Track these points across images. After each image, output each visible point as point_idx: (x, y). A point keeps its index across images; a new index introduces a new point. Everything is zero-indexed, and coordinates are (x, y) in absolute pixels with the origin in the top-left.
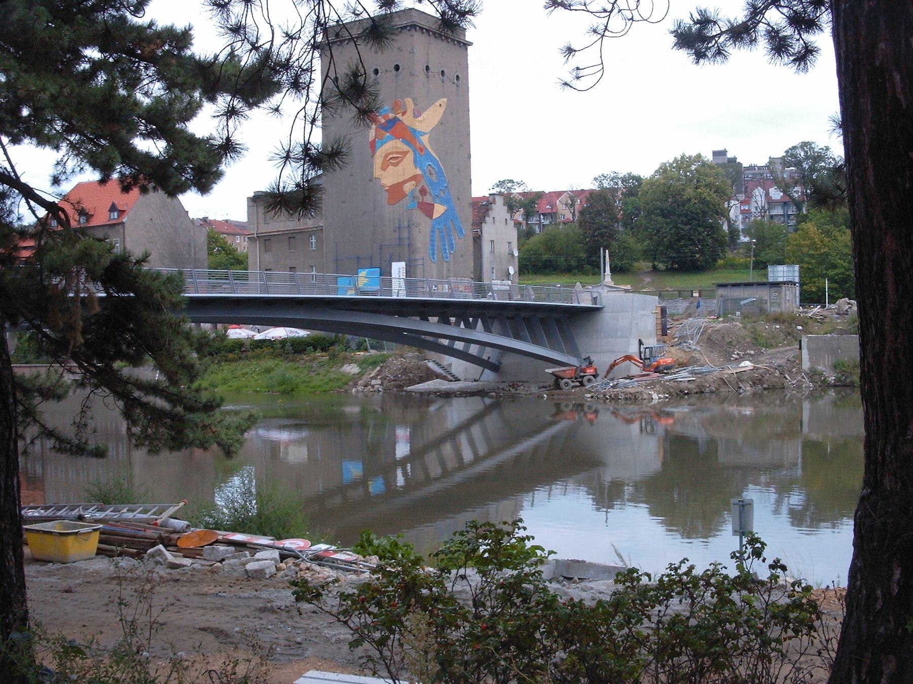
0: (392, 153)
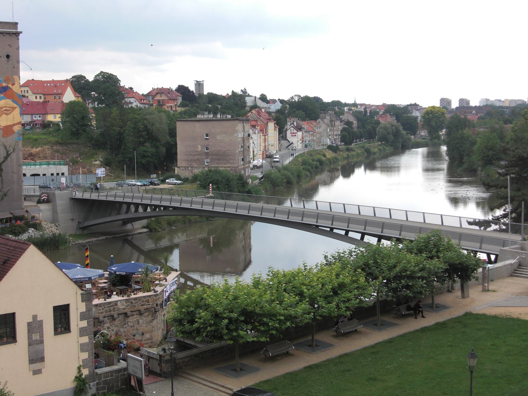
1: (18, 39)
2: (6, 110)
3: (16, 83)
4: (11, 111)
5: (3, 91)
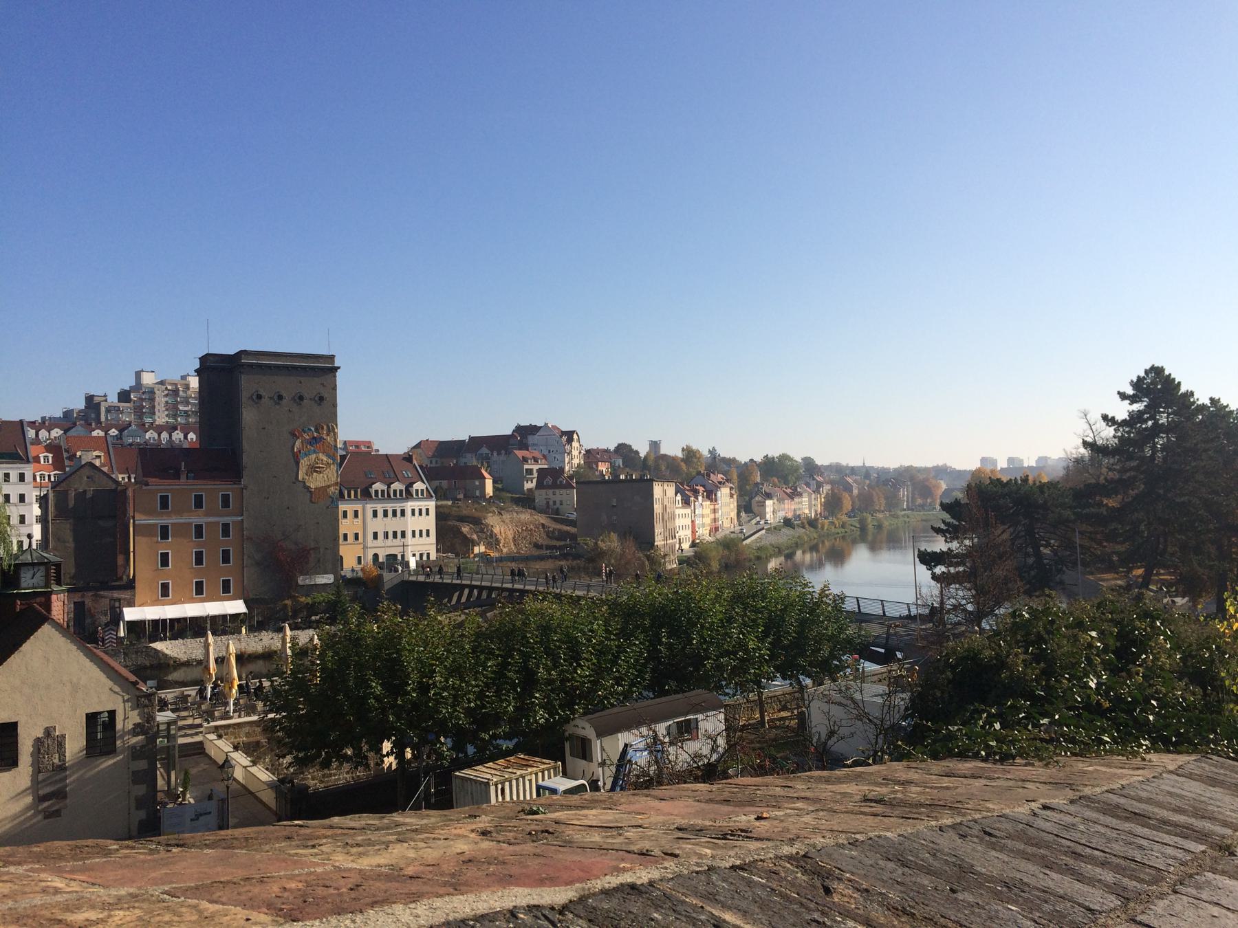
1: (335, 376)
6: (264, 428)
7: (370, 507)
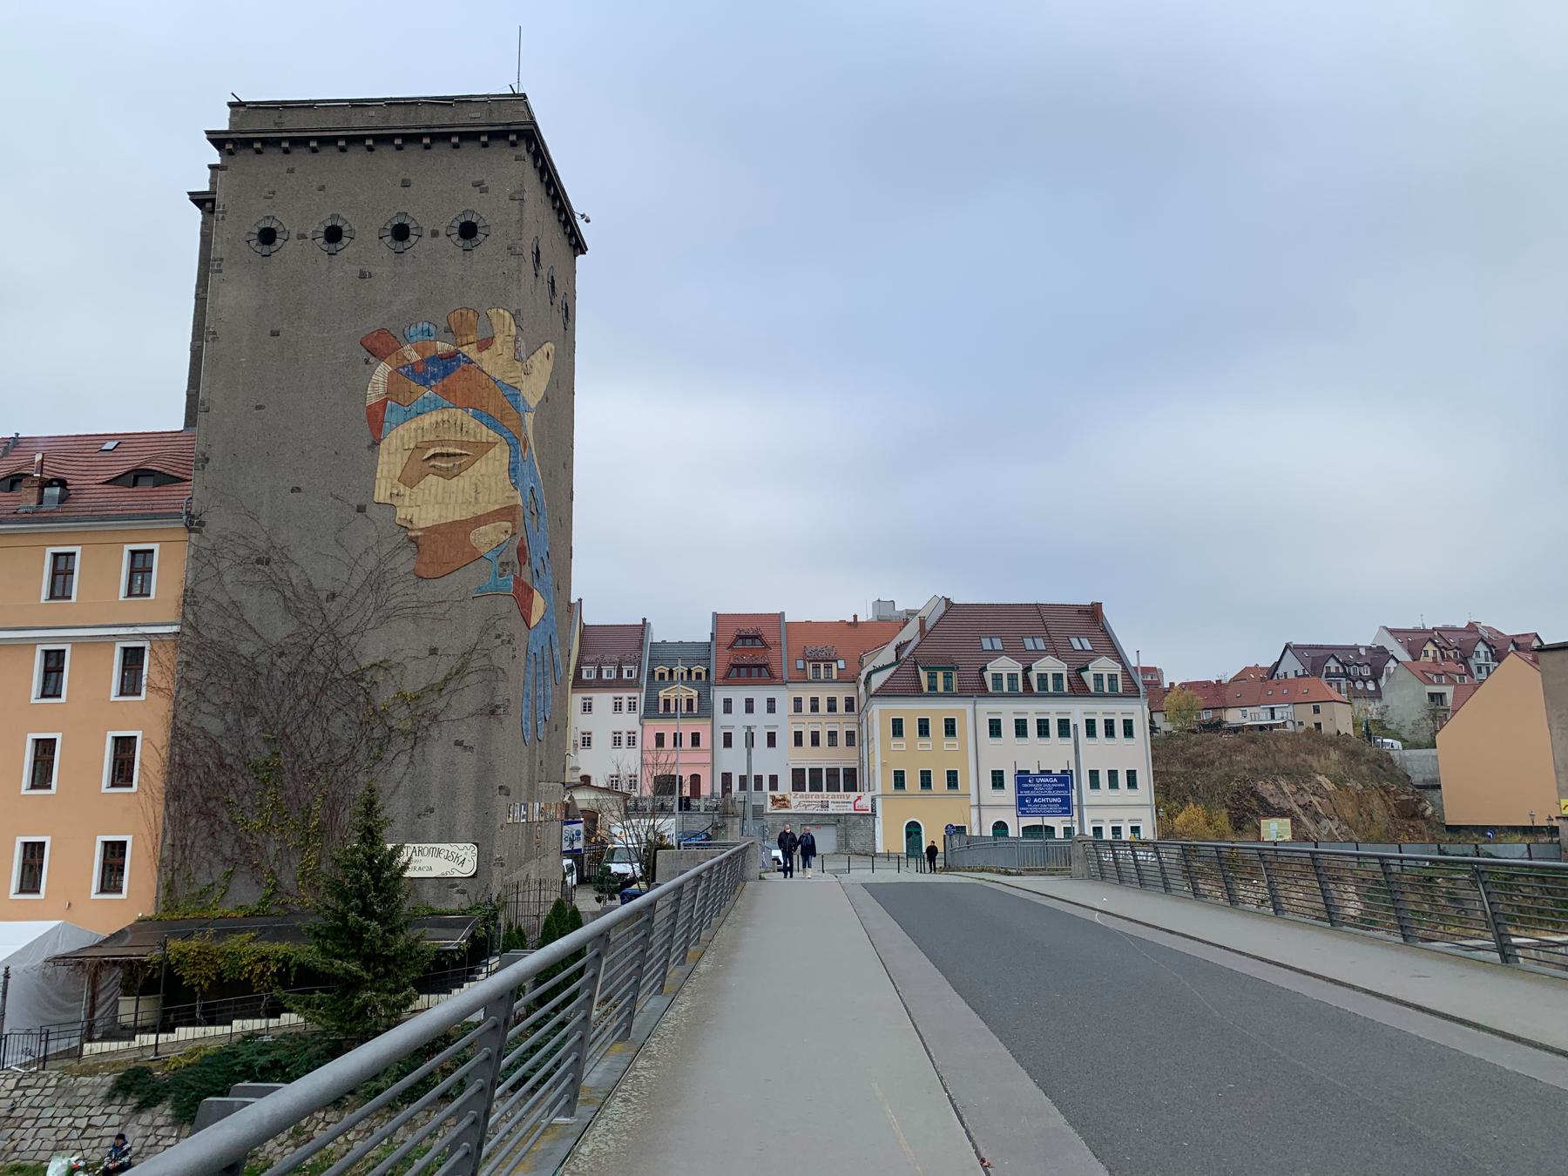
0: (442, 443)
2: (442, 455)
3: (498, 341)
4: (465, 459)
5: (434, 377)
6: (275, 334)
7: (988, 709)
